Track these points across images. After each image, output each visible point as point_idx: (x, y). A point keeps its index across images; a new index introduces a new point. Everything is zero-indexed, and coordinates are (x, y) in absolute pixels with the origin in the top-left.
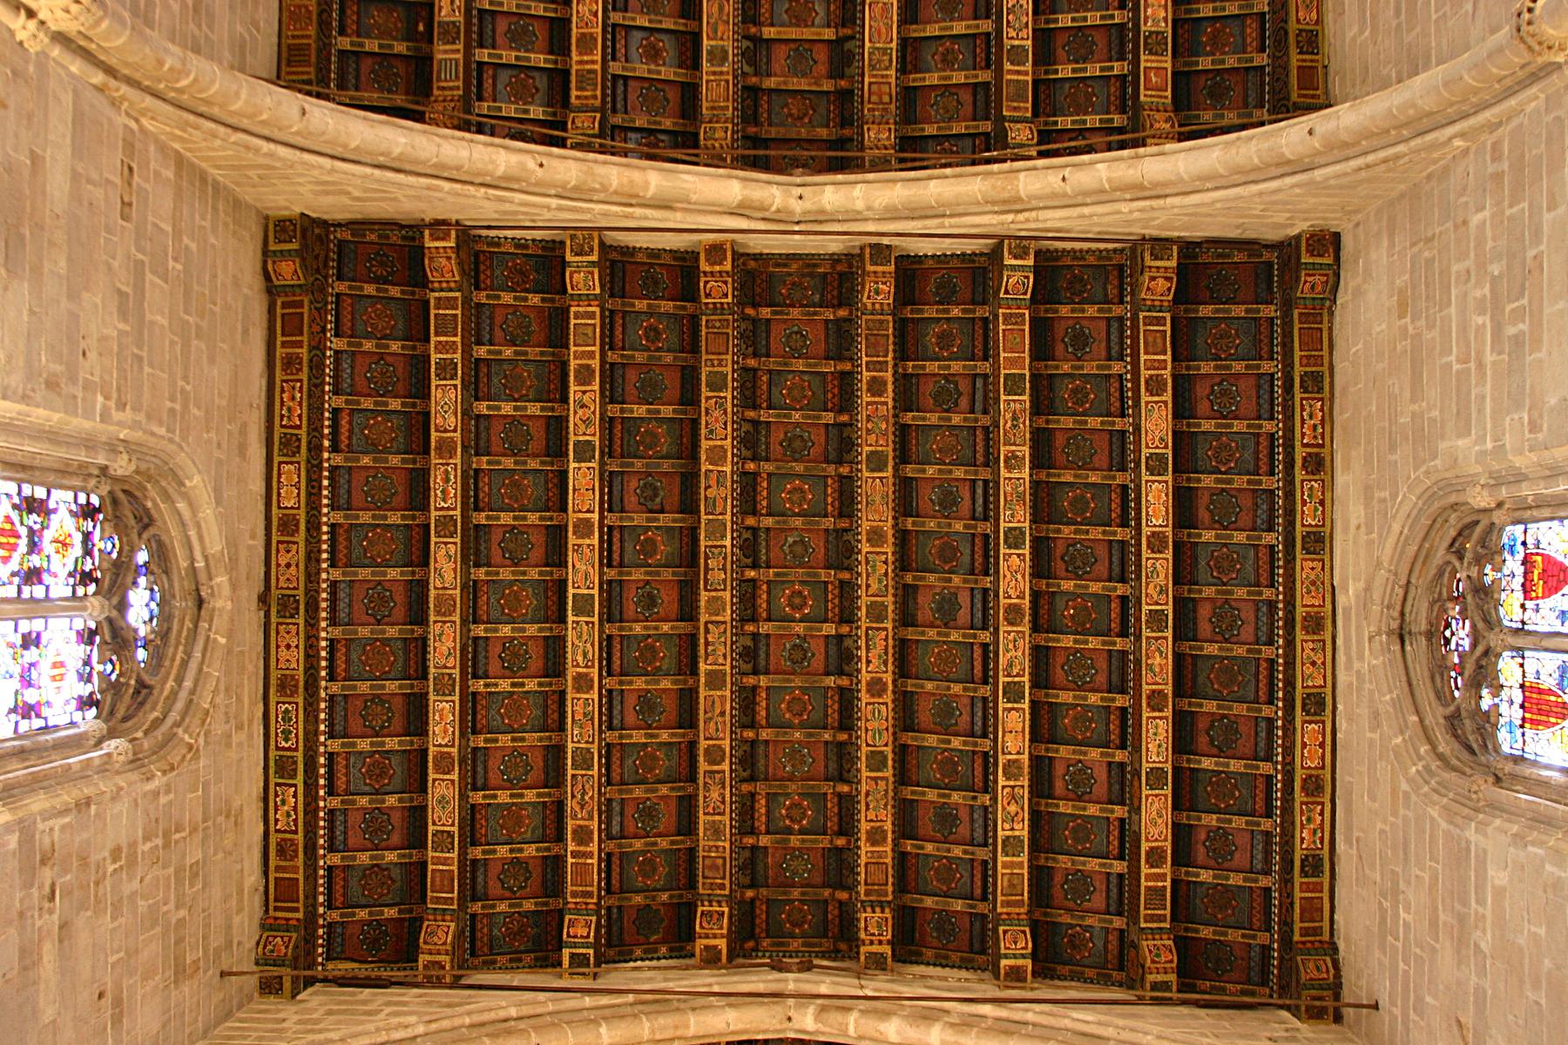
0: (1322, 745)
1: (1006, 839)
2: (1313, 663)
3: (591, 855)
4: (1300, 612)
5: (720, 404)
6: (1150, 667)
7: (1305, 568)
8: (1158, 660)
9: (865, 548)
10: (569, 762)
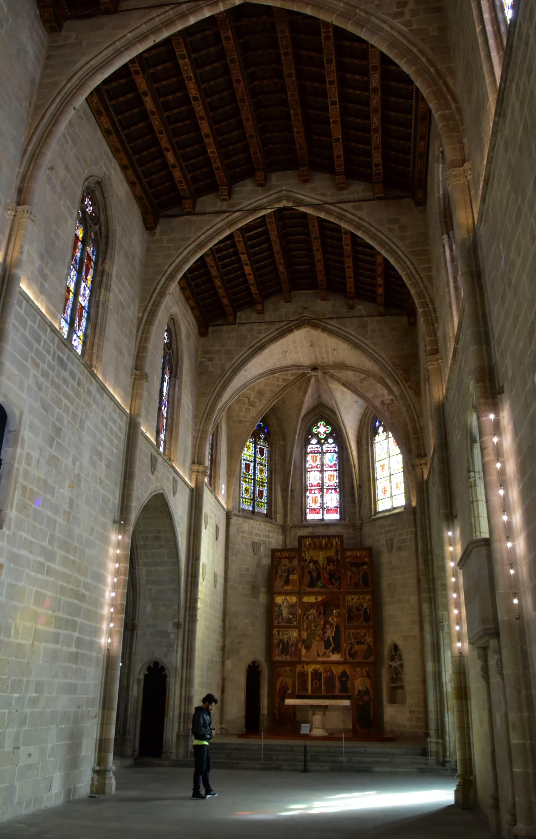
0: (101, 123)
1: (185, 58)
2: (113, 142)
3: (324, 32)
4: (122, 152)
6: (158, 121)
7: (126, 162)
8: (156, 123)
9: (250, 116)
10: (334, 60)
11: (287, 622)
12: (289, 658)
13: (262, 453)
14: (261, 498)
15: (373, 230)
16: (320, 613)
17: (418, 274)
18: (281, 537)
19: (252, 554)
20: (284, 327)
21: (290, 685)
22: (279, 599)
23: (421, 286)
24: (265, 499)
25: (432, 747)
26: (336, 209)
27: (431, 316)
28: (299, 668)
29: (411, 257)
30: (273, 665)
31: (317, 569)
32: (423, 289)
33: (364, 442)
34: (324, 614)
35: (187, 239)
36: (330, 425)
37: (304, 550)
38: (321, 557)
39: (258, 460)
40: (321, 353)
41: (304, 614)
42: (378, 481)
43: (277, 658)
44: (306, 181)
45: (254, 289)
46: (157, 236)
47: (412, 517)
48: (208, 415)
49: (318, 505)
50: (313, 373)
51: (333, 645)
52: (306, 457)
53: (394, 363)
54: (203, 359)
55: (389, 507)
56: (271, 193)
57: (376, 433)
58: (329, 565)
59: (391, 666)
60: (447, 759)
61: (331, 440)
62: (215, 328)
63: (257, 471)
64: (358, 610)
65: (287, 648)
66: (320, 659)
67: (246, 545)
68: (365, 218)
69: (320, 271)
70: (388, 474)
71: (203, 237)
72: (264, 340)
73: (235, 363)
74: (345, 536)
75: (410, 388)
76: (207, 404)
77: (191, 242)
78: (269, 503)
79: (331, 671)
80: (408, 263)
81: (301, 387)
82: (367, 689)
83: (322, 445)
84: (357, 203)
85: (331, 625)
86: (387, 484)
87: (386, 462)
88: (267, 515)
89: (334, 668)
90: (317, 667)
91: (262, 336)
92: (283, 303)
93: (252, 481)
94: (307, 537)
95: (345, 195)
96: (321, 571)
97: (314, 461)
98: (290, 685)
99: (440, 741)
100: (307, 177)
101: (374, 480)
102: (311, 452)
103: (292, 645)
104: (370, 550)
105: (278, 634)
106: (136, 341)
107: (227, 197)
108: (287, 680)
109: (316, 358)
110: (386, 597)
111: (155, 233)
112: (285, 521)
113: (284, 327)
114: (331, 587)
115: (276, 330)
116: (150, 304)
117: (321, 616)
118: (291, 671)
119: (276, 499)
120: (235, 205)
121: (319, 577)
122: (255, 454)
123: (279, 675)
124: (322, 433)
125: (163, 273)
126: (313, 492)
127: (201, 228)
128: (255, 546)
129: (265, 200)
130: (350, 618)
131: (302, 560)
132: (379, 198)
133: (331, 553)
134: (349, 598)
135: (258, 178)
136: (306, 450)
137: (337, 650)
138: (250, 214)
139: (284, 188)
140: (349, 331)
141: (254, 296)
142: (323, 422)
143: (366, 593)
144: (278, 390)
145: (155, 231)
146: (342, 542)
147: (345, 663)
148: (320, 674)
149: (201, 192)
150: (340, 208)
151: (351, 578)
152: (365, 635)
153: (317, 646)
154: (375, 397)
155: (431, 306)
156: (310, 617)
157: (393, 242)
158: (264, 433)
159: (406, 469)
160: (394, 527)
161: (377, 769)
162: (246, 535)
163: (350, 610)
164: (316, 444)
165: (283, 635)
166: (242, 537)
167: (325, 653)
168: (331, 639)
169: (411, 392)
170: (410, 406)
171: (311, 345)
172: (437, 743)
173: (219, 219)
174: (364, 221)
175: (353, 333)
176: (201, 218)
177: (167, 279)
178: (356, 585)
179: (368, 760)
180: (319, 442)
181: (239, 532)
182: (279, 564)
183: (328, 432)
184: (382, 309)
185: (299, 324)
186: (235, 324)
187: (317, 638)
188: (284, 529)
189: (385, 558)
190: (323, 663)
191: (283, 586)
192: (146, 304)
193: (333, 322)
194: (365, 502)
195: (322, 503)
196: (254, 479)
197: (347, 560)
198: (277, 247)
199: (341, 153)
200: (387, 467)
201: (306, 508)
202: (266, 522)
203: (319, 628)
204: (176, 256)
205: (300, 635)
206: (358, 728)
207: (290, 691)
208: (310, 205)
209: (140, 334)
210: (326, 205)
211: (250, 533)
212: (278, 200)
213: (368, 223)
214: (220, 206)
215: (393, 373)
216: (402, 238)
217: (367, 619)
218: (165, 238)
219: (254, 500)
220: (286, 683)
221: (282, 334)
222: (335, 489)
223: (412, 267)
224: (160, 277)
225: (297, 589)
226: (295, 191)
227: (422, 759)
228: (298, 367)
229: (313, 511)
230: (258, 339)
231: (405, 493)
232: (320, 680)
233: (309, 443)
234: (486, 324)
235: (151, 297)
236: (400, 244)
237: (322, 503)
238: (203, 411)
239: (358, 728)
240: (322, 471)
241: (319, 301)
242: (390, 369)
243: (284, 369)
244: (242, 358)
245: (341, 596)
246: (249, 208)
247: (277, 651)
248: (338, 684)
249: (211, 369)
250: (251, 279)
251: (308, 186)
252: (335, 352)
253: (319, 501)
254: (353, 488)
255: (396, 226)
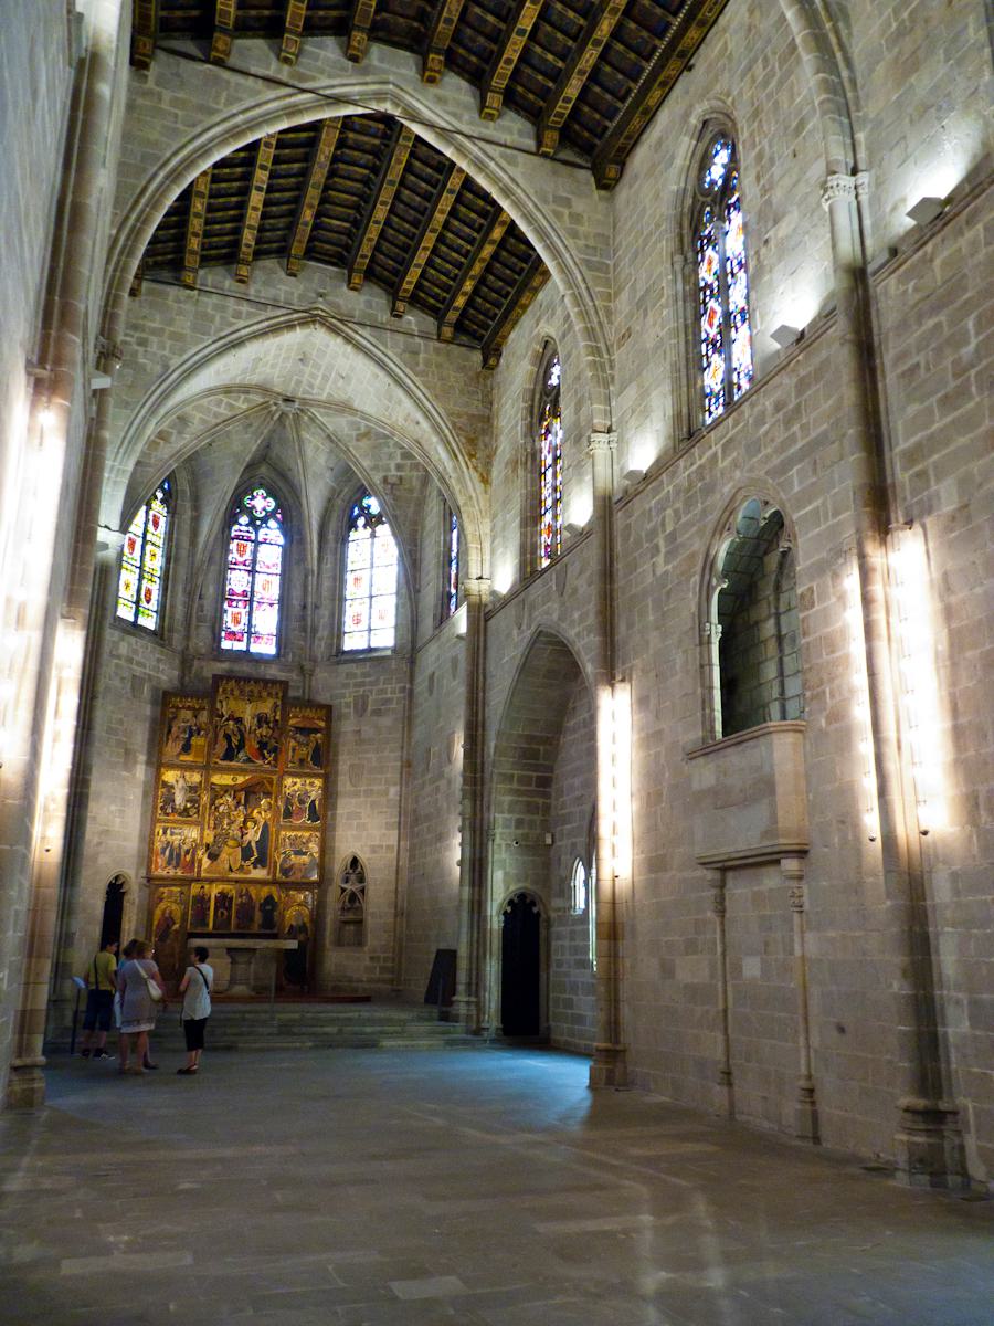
5: (450, 11)
11: (180, 814)
12: (179, 873)
13: (156, 524)
14: (148, 602)
15: (531, 205)
16: (239, 803)
17: (592, 300)
18: (176, 673)
19: (130, 695)
20: (282, 319)
21: (177, 916)
22: (170, 776)
23: (596, 320)
24: (153, 605)
25: (462, 1010)
26: (475, 150)
27: (603, 370)
28: (195, 889)
29: (584, 269)
30: (152, 881)
31: (240, 730)
32: (596, 325)
33: (331, 537)
34: (245, 805)
35: (212, 112)
36: (275, 498)
37: (220, 697)
38: (248, 712)
39: (149, 537)
40: (313, 376)
41: (212, 803)
42: (348, 603)
43: (161, 872)
44: (432, 80)
45: (248, 237)
46: (150, 84)
47: (405, 667)
48: (130, 442)
49: (241, 626)
50: (283, 406)
51: (256, 855)
52: (228, 544)
53: (454, 424)
54: (128, 339)
55: (363, 646)
56: (368, 79)
57: (353, 525)
58: (260, 726)
59: (343, 890)
60: (484, 1025)
61: (272, 523)
62: (154, 286)
63: (148, 557)
64: (302, 802)
65: (179, 855)
66: (232, 875)
67: (123, 679)
68: (520, 181)
69: (370, 240)
70: (367, 594)
71: (240, 118)
72: (243, 332)
73: (187, 360)
74: (291, 684)
75: (475, 468)
76: (132, 424)
77: (218, 119)
78: (162, 612)
79: (248, 894)
80: (579, 278)
81: (250, 425)
82: (304, 924)
83: (257, 529)
84: (509, 151)
85: (256, 823)
86: (364, 610)
87: (365, 575)
88: (154, 633)
89: (253, 891)
90: (226, 887)
91: (241, 324)
92: (282, 274)
93: (138, 571)
94: (229, 678)
95: (490, 130)
96: (246, 735)
97: (241, 552)
98: (177, 916)
99: (473, 999)
100: (437, 75)
101: (342, 599)
102: (237, 537)
103: (187, 852)
104: (328, 711)
105: (165, 833)
106: (104, 281)
107: (293, 57)
108: (174, 907)
109: (299, 383)
110: (344, 783)
111: (146, 77)
112: (187, 648)
113: (282, 319)
114: (260, 762)
115: (268, 320)
116: (134, 216)
117: (241, 808)
118: (182, 893)
119: (173, 607)
120: (303, 78)
121: (241, 746)
122: (146, 524)
123: (161, 900)
124: (259, 509)
125: (162, 162)
126: (234, 604)
127: (239, 100)
128: (136, 682)
129: (357, 88)
130: (288, 814)
131: (214, 713)
132: (545, 155)
133: (266, 707)
134: (289, 781)
135: (355, 44)
136: (230, 529)
137: (261, 862)
138: (328, 104)
139: (391, 78)
140: (390, 353)
141: (244, 249)
142: (261, 491)
143: (316, 776)
144: (215, 421)
145: (146, 72)
146: (285, 692)
147: (274, 882)
148: (231, 899)
149: (243, 28)
150: (481, 149)
151: (294, 750)
152: (309, 840)
153: (229, 855)
154: (376, 468)
155: (606, 356)
156: (221, 809)
157: (559, 236)
158: (164, 491)
159: (404, 591)
160: (372, 679)
161: (386, 1043)
162: (122, 662)
163: (288, 801)
164: (247, 525)
165: (172, 834)
166: (117, 665)
167: (242, 866)
168: (253, 845)
169: (475, 476)
170: (471, 498)
171: (301, 360)
172: (468, 1003)
173: (271, 94)
174: (518, 185)
175: (395, 359)
176: (235, 78)
177: (167, 177)
178: (302, 761)
179: (368, 1029)
180: (252, 523)
181: (112, 656)
182: (175, 718)
183: (269, 509)
184: (448, 332)
185: (310, 319)
186: (192, 288)
187: (231, 843)
188: (186, 662)
189: (347, 727)
190: (237, 881)
191: (180, 754)
192: (125, 212)
193: (366, 332)
194: (323, 633)
195: (250, 625)
196: (141, 568)
197: (292, 722)
198: (319, 175)
199: (515, 58)
200: (365, 583)
201: (221, 630)
202: (157, 643)
203: (235, 826)
204: (189, 137)
205: (202, 838)
206: (285, 983)
207: (176, 926)
208: (431, 126)
209: (111, 268)
210: (459, 136)
211: (130, 660)
212: (379, 97)
213: (524, 191)
214: (273, 68)
215: (451, 439)
216: (574, 235)
217: (314, 815)
218: (167, 95)
219: (137, 603)
220: (171, 912)
221: (275, 330)
222: (271, 605)
223: (583, 286)
224: (155, 168)
225: (201, 761)
226: (411, 92)
227: (443, 1026)
228: (264, 389)
229: (232, 635)
230: (236, 328)
231: (396, 627)
232: (229, 909)
233: (237, 522)
234: (878, 425)
235: (136, 202)
236: (569, 242)
237: (250, 625)
238: (122, 434)
239: (285, 983)
240: (253, 572)
241: (345, 288)
242: (447, 431)
243: (245, 389)
244: (201, 355)
245: (275, 778)
246: (328, 92)
247: (159, 860)
248: (258, 916)
249: (142, 361)
250: (253, 218)
251: (433, 90)
252: (341, 383)
253: (244, 619)
254: (304, 607)
255: (566, 212)
